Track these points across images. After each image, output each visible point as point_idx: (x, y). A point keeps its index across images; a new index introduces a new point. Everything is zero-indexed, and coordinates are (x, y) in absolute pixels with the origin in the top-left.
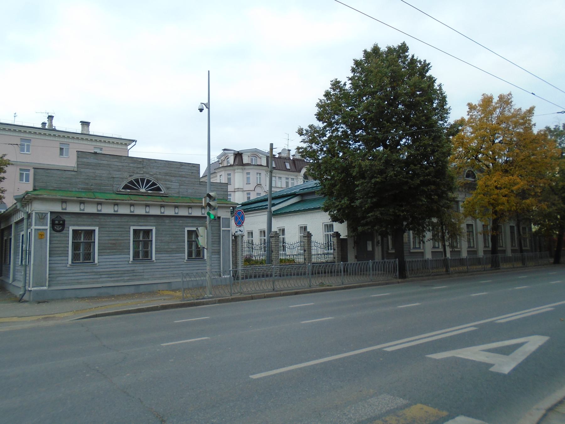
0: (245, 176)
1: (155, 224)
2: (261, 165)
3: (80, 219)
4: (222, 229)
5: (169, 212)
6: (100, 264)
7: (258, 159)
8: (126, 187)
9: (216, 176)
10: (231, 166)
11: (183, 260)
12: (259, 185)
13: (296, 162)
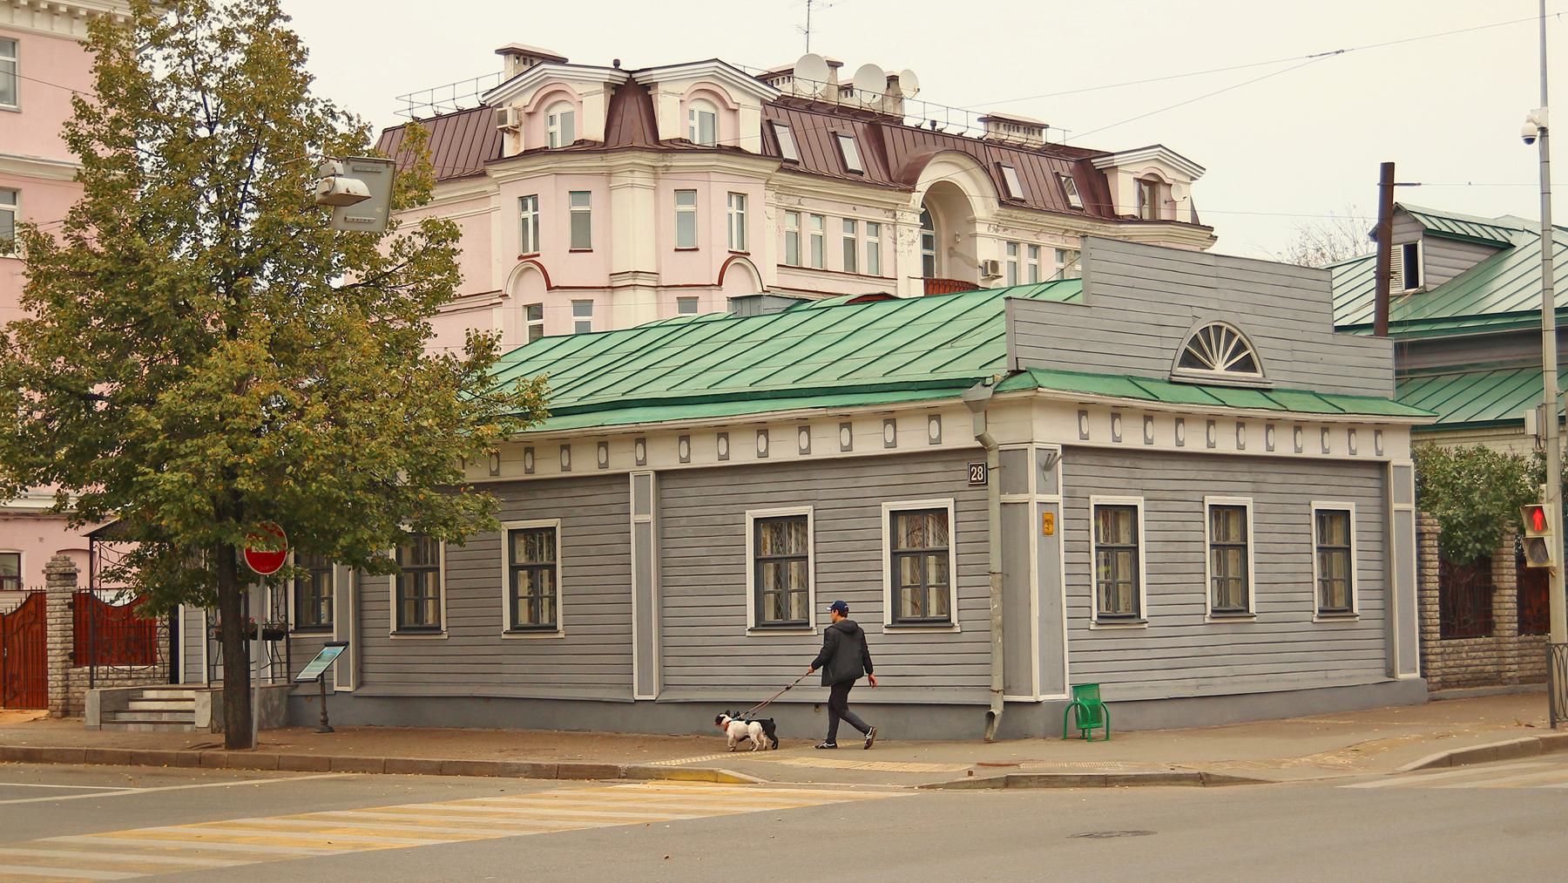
0: (671, 206)
1: (1249, 487)
2: (737, 151)
3: (1107, 472)
4: (1395, 506)
5: (1284, 446)
6: (1154, 621)
7: (724, 118)
8: (1189, 360)
9: (486, 196)
10: (583, 147)
11: (1308, 616)
12: (739, 256)
13: (886, 130)
